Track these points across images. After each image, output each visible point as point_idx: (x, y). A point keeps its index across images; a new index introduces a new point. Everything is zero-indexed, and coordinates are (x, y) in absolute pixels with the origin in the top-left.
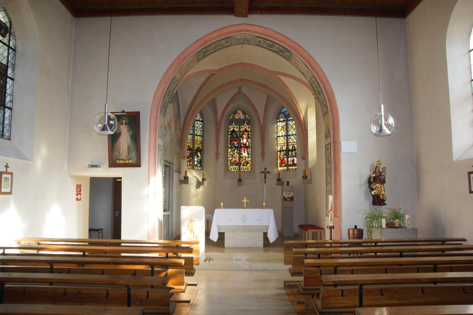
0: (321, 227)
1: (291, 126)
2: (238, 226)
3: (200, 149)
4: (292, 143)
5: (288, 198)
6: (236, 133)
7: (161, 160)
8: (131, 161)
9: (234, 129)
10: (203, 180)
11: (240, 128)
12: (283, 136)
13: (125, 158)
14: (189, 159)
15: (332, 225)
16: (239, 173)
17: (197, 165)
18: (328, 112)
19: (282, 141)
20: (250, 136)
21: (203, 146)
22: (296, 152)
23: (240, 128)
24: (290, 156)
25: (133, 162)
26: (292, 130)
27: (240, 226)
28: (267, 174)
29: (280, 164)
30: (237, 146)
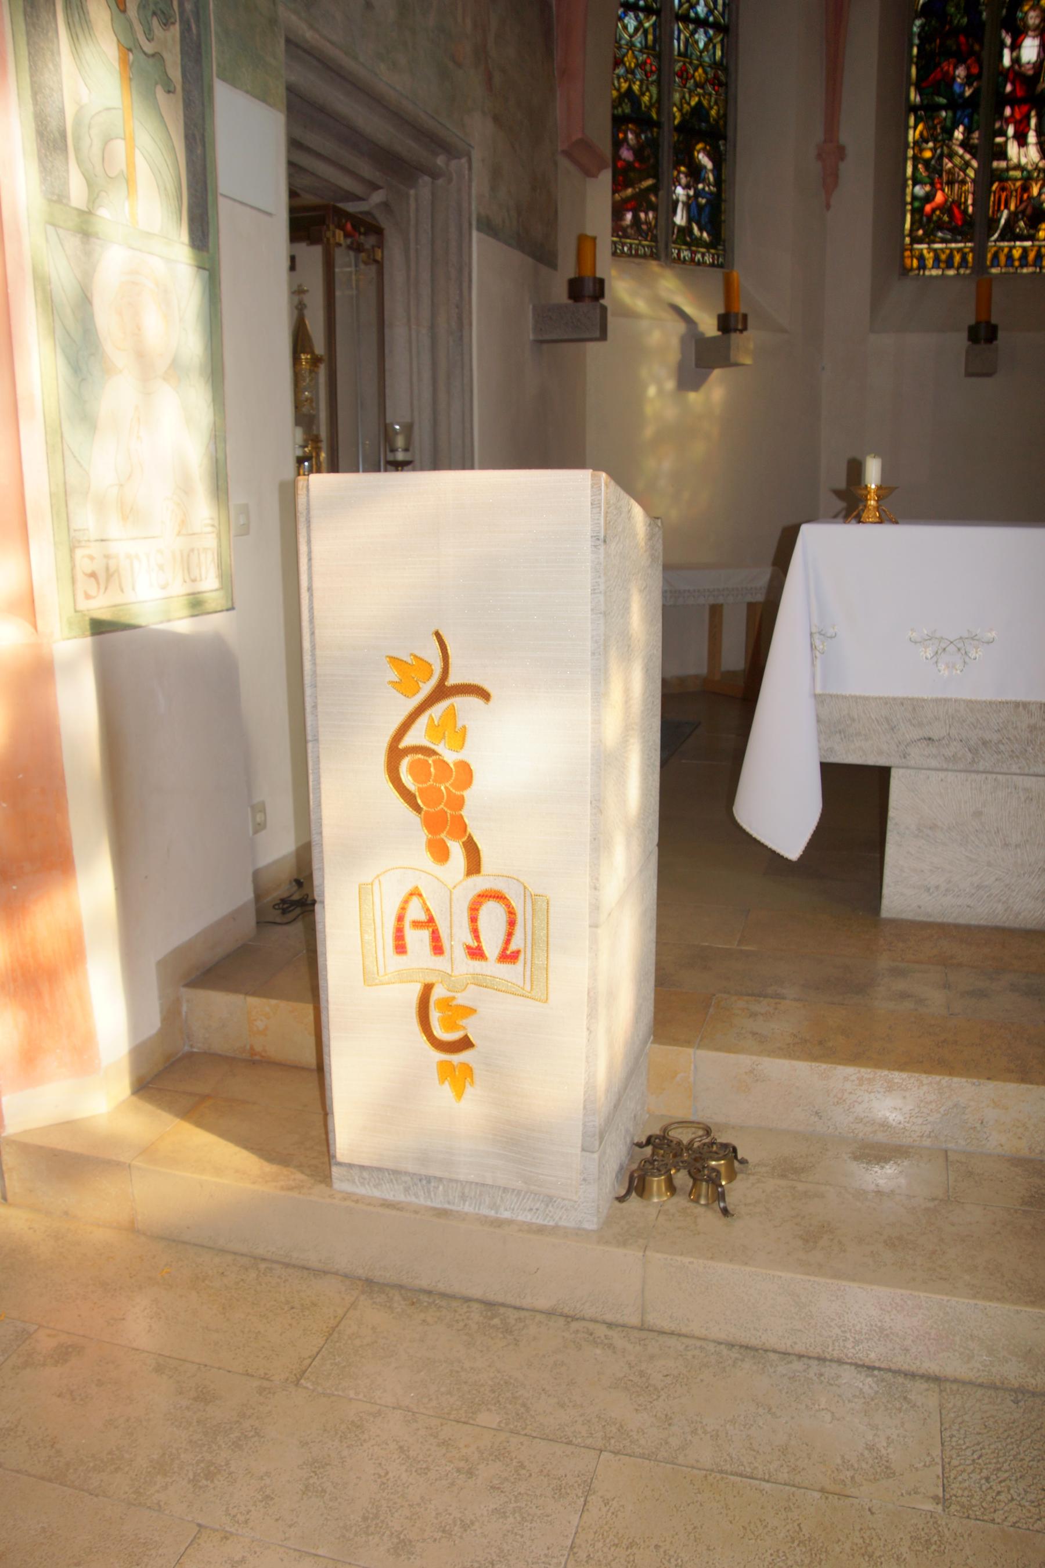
3: (708, 121)
10: (728, 323)
17: (686, 231)
21: (727, 102)
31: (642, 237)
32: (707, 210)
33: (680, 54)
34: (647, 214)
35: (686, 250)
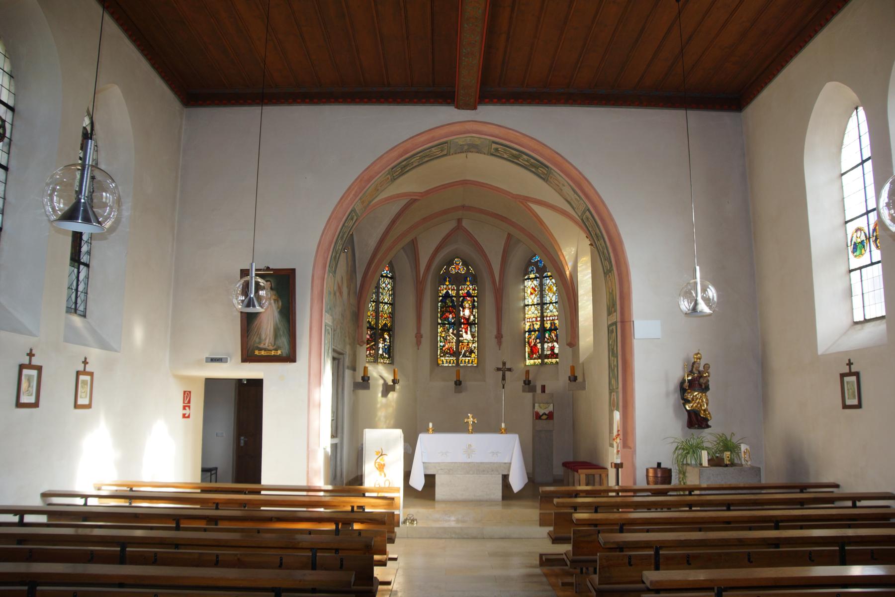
0: (602, 465)
1: (549, 287)
2: (459, 463)
4: (550, 317)
5: (543, 415)
6: (451, 299)
7: (328, 350)
8: (279, 352)
9: (447, 292)
11: (458, 290)
12: (534, 305)
13: (269, 346)
15: (619, 461)
16: (457, 371)
18: (613, 270)
19: (533, 313)
20: (476, 304)
21: (393, 322)
22: (557, 332)
23: (458, 290)
24: (546, 340)
25: (284, 354)
26: (551, 295)
27: (462, 463)
28: (508, 374)
29: (529, 354)
30: (453, 321)
32: (387, 349)
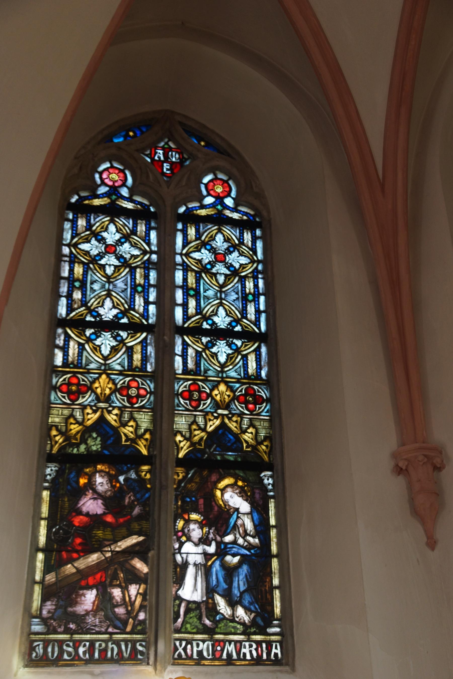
14: (99, 549)
31: (115, 627)
33: (186, 371)
34: (124, 589)
35: (204, 641)
